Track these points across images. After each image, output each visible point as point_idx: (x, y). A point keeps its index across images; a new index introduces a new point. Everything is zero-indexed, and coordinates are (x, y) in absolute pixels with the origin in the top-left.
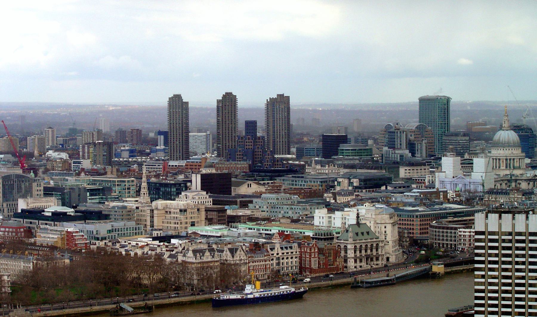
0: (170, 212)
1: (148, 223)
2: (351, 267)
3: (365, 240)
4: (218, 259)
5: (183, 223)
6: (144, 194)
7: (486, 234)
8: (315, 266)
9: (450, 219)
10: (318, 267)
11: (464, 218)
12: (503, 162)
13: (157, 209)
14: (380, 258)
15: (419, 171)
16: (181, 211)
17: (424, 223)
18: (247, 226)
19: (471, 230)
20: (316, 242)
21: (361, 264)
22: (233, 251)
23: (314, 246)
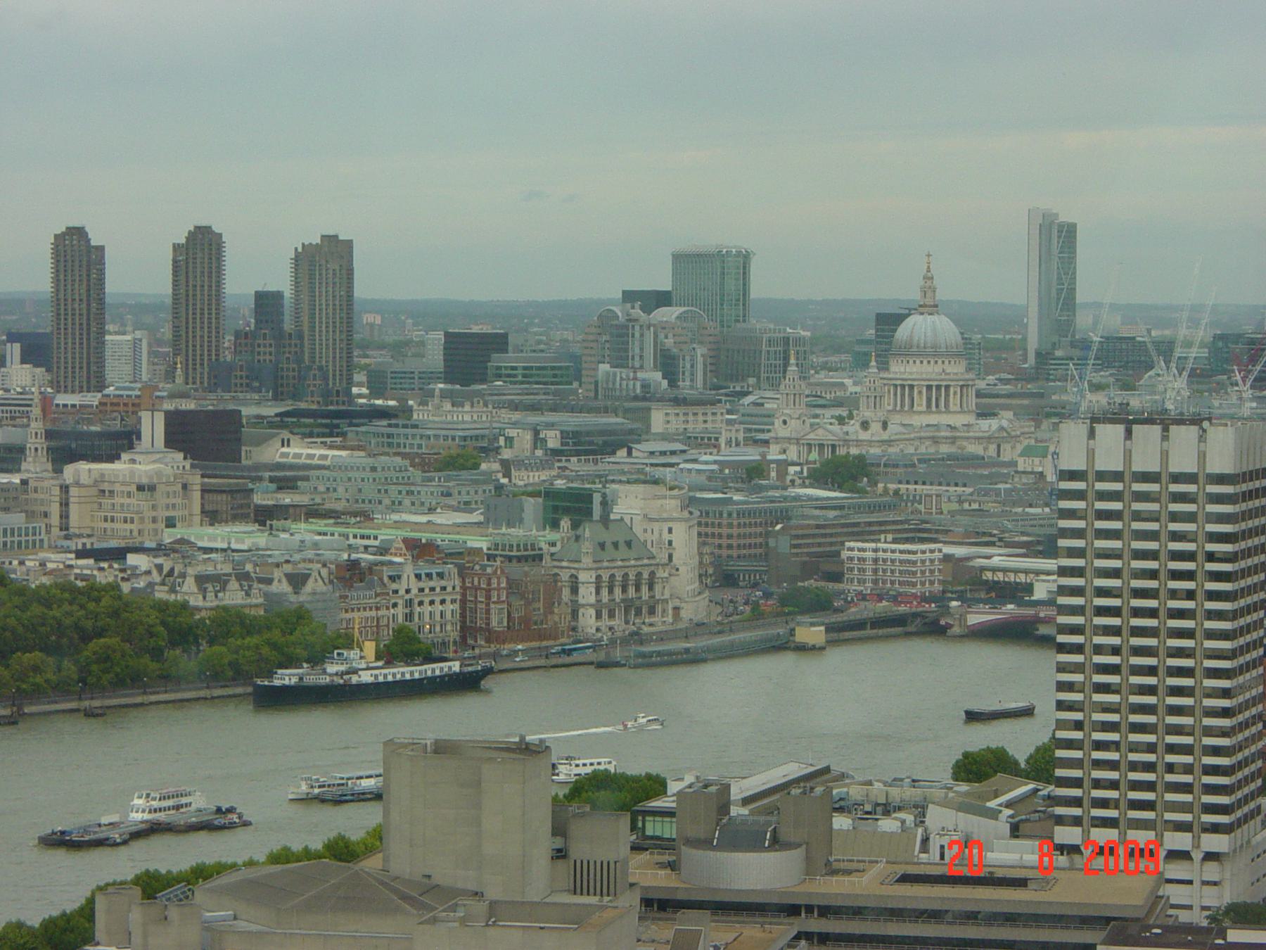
1: (55, 520)
3: (622, 560)
5: (146, 520)
6: (36, 449)
8: (497, 621)
10: (509, 627)
12: (920, 392)
13: (77, 484)
14: (659, 608)
16: (140, 488)
17: (748, 530)
18: (313, 527)
19: (880, 545)
20: (502, 562)
22: (297, 581)
23: (499, 572)
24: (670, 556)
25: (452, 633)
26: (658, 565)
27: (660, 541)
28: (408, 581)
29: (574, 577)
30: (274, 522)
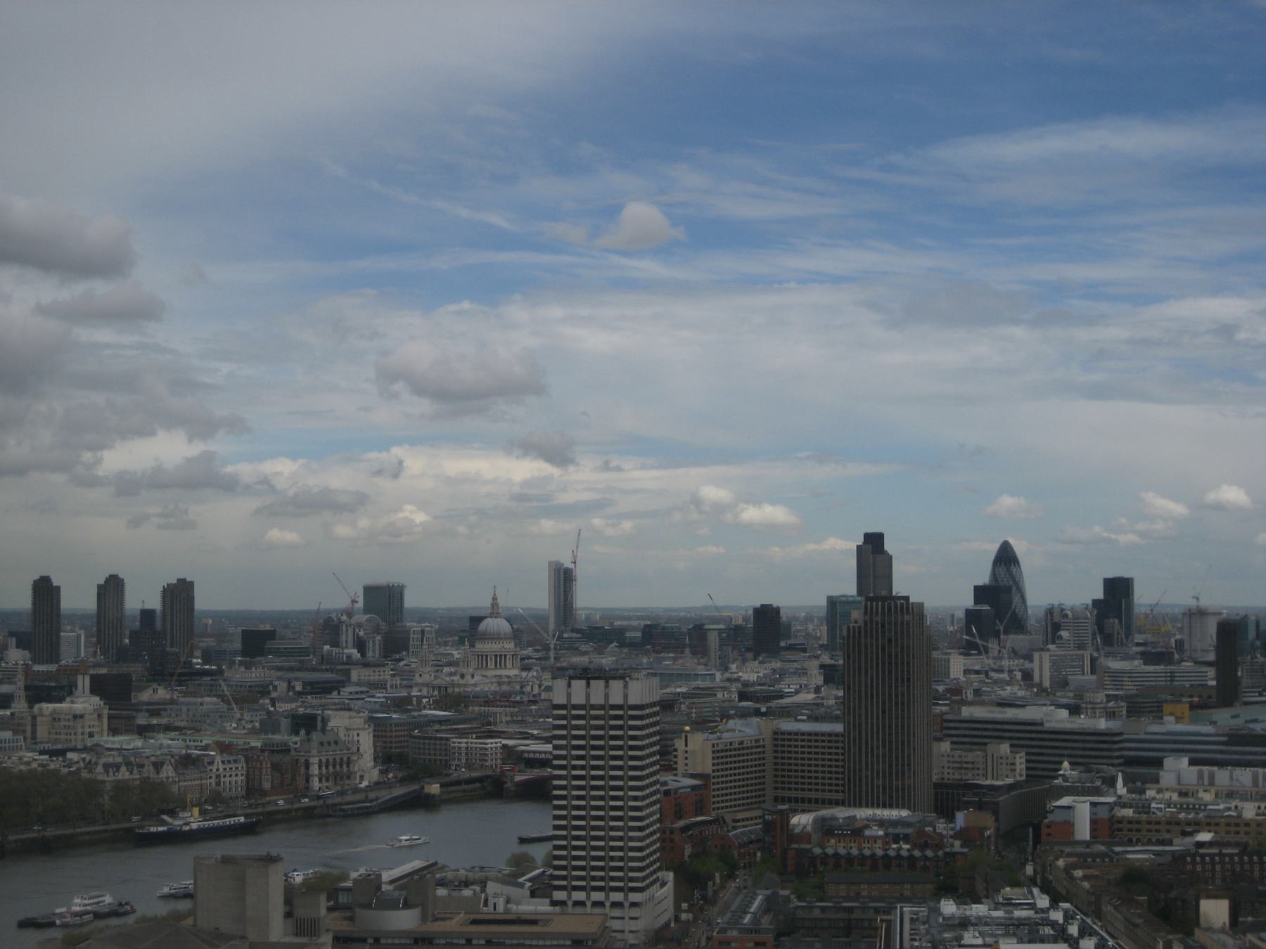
0: (59, 719)
1: (29, 734)
2: (315, 788)
4: (138, 776)
6: (20, 696)
7: (569, 707)
8: (267, 786)
9: (437, 727)
10: (272, 787)
11: (455, 727)
12: (491, 659)
13: (42, 715)
14: (352, 777)
15: (382, 673)
16: (75, 717)
19: (469, 740)
21: (327, 784)
22: (158, 766)
23: (267, 759)
24: (358, 748)
25: (241, 791)
26: (352, 754)
27: (353, 741)
28: (218, 765)
30: (147, 734)
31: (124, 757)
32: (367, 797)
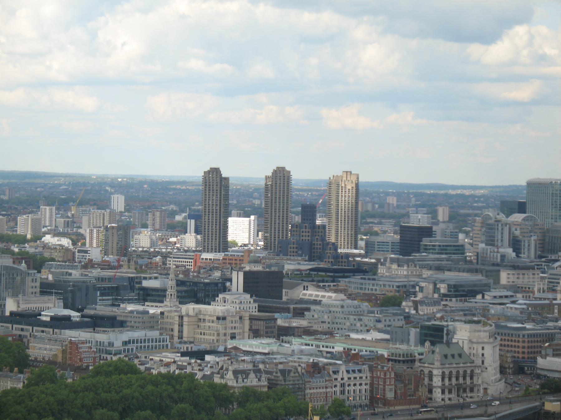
0: (204, 320)
1: (176, 333)
5: (221, 335)
6: (171, 295)
8: (390, 395)
10: (395, 398)
13: (188, 315)
14: (476, 389)
16: (218, 318)
17: (533, 344)
18: (303, 341)
20: (392, 364)
21: (450, 396)
23: (390, 370)
25: (365, 401)
26: (475, 366)
27: (477, 355)
28: (343, 373)
29: (430, 372)
30: (284, 338)
31: (254, 363)
32: (486, 412)
